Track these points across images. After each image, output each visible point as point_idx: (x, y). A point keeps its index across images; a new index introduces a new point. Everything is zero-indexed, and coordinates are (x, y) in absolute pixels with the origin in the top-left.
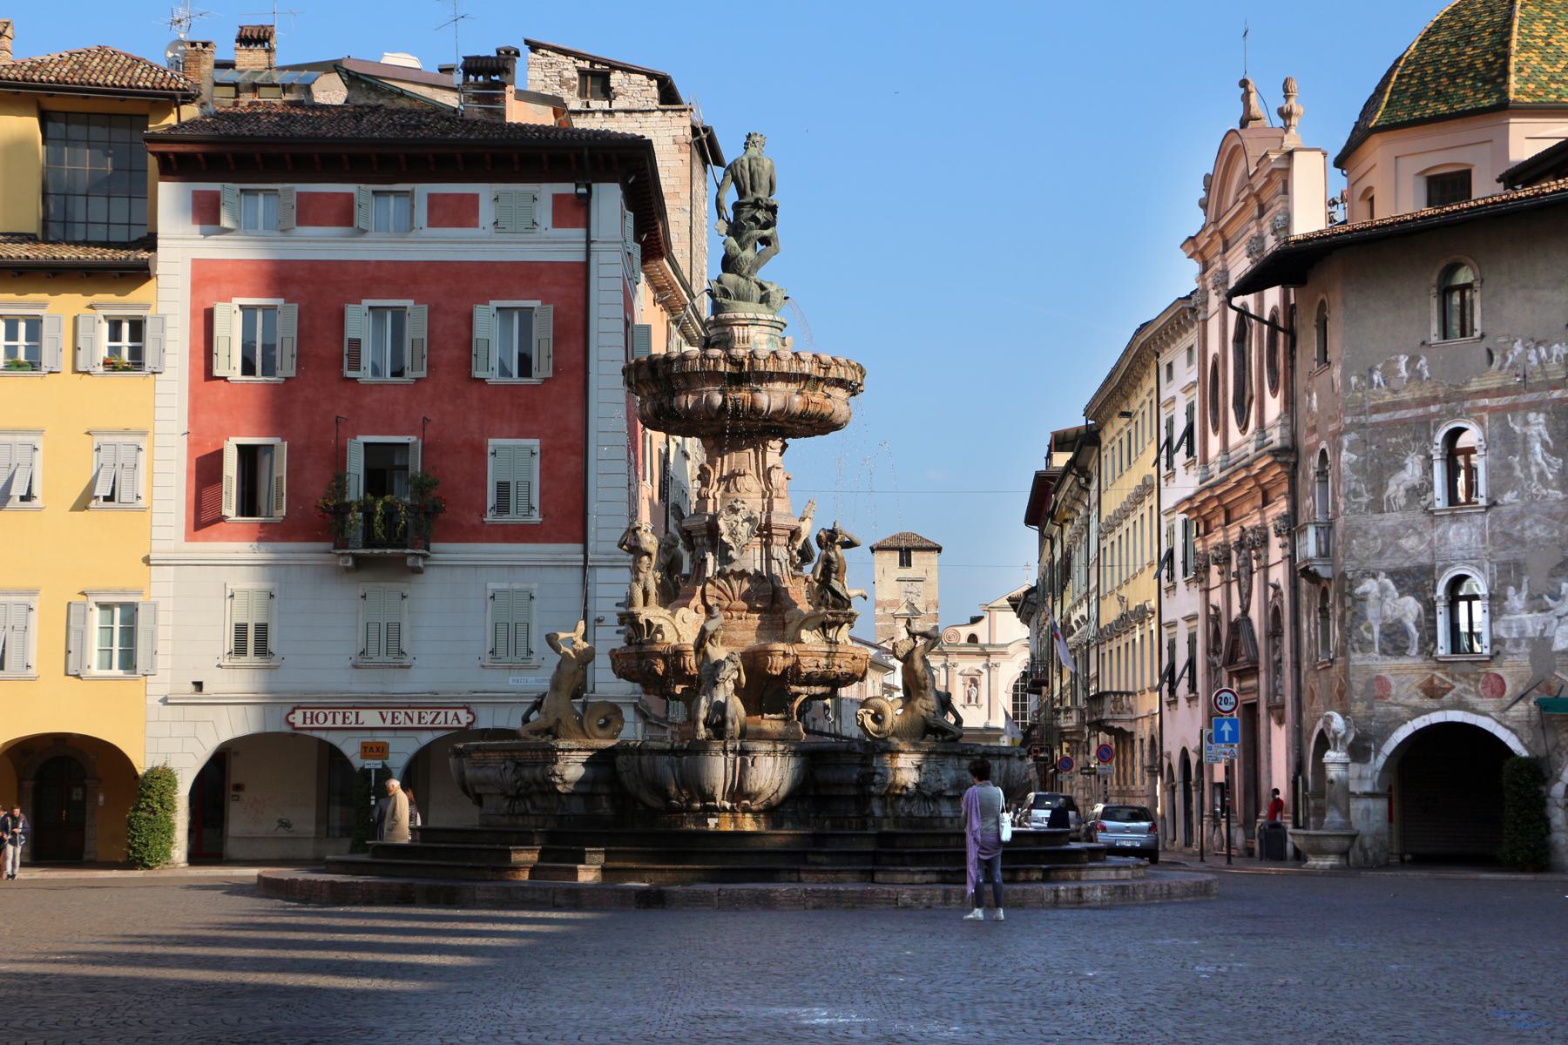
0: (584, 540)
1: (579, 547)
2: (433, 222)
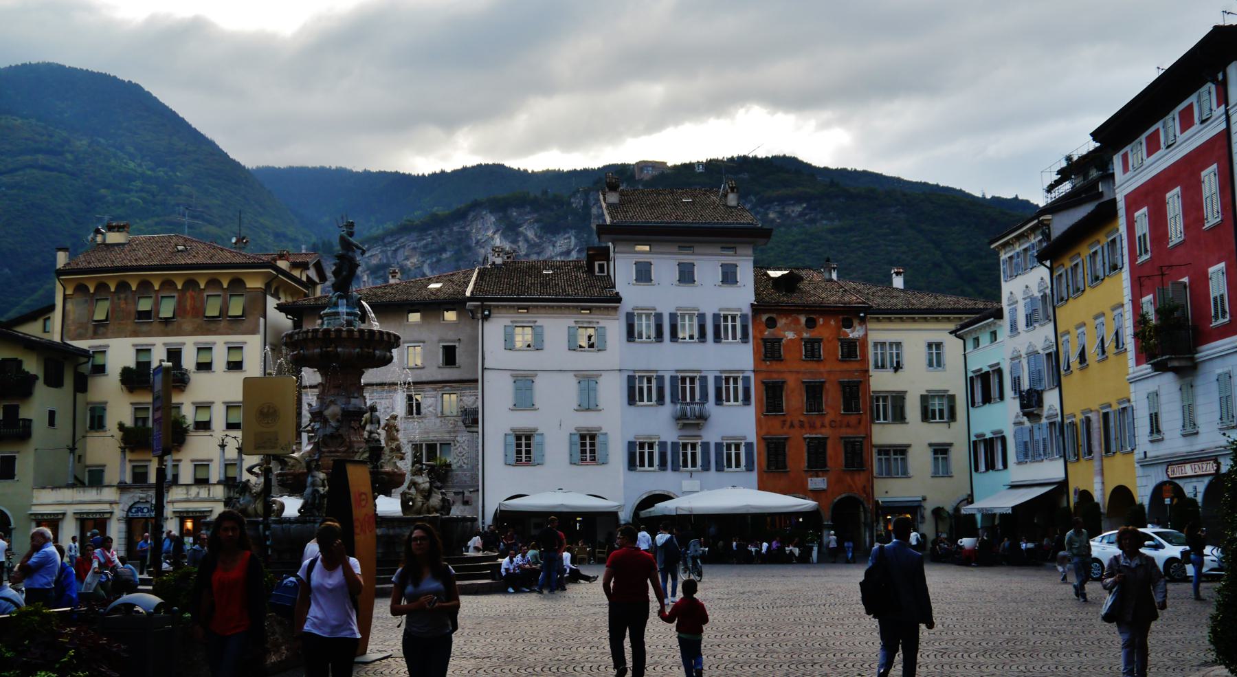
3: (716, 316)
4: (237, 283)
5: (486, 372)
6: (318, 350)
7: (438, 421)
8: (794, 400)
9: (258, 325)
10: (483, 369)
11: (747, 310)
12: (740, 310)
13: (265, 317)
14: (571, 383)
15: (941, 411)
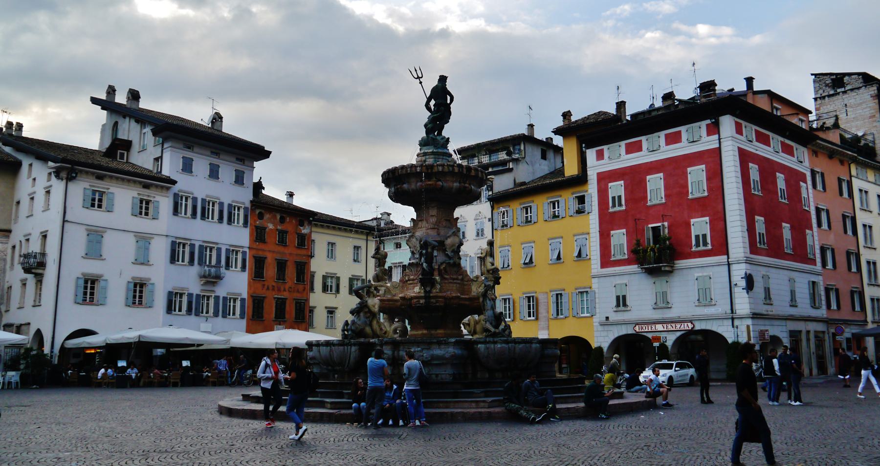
0: (728, 254)
1: (726, 257)
2: (667, 144)
3: (230, 206)
5: (66, 224)
6: (456, 185)
8: (270, 271)
11: (248, 205)
12: (243, 203)
14: (131, 240)
15: (331, 286)
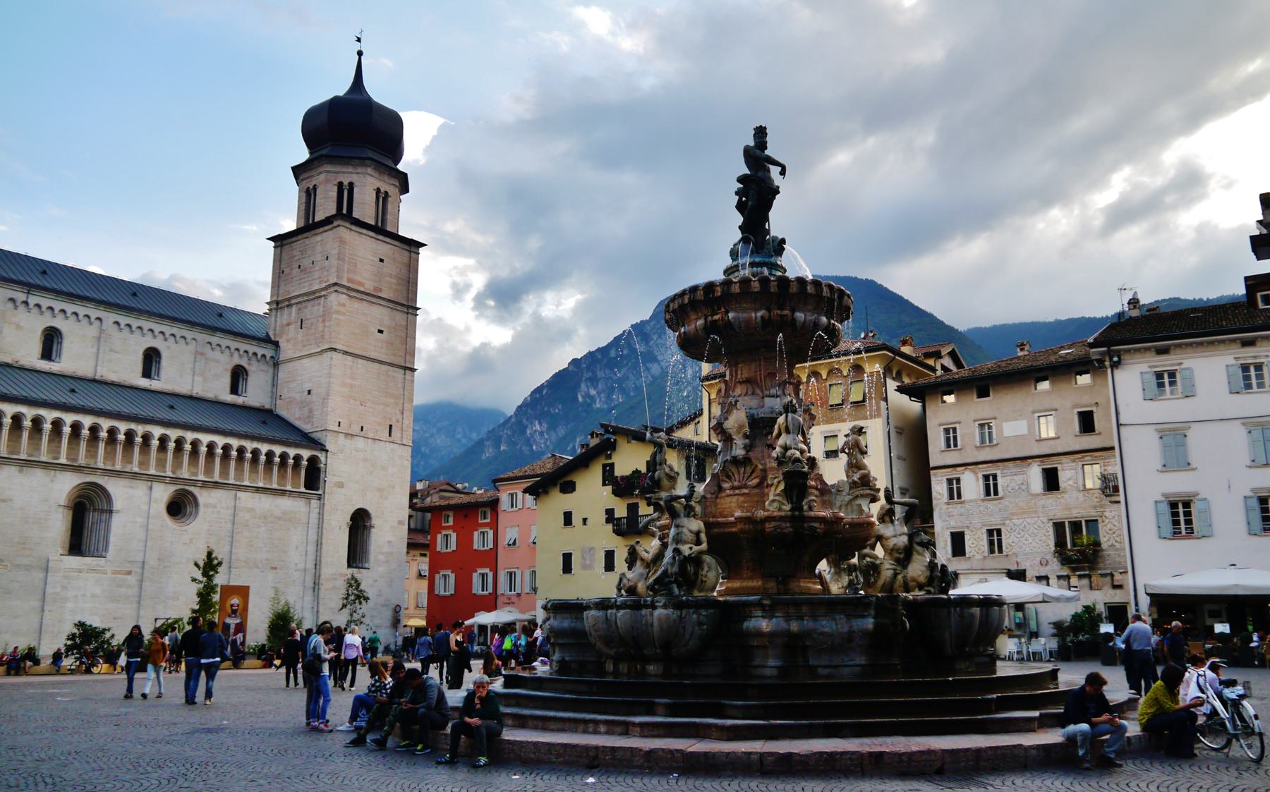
4: (858, 368)
5: (1122, 429)
6: (700, 322)
7: (1081, 494)
9: (878, 409)
10: (1119, 425)
13: (886, 400)
14: (1239, 431)
